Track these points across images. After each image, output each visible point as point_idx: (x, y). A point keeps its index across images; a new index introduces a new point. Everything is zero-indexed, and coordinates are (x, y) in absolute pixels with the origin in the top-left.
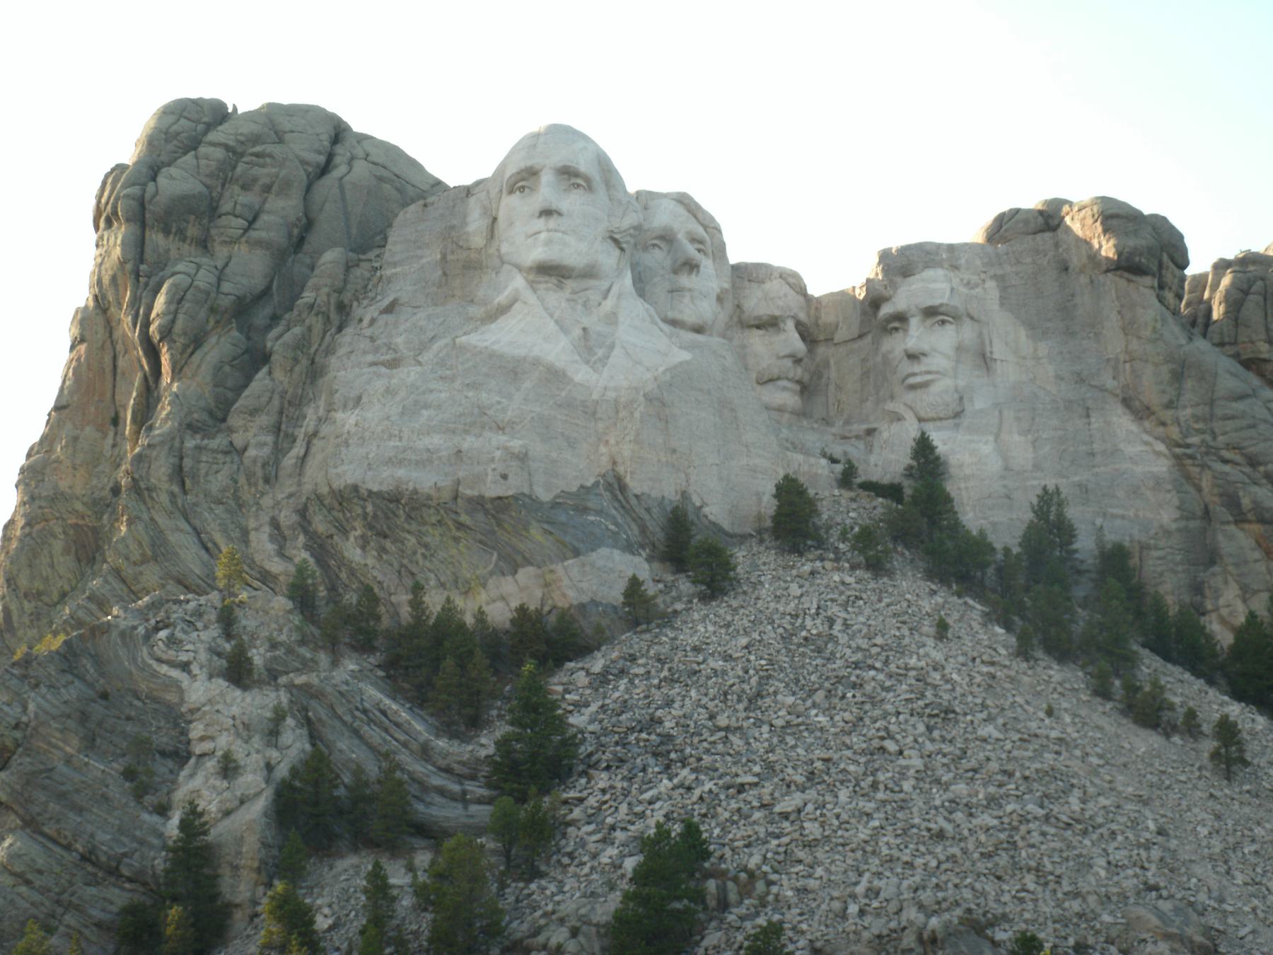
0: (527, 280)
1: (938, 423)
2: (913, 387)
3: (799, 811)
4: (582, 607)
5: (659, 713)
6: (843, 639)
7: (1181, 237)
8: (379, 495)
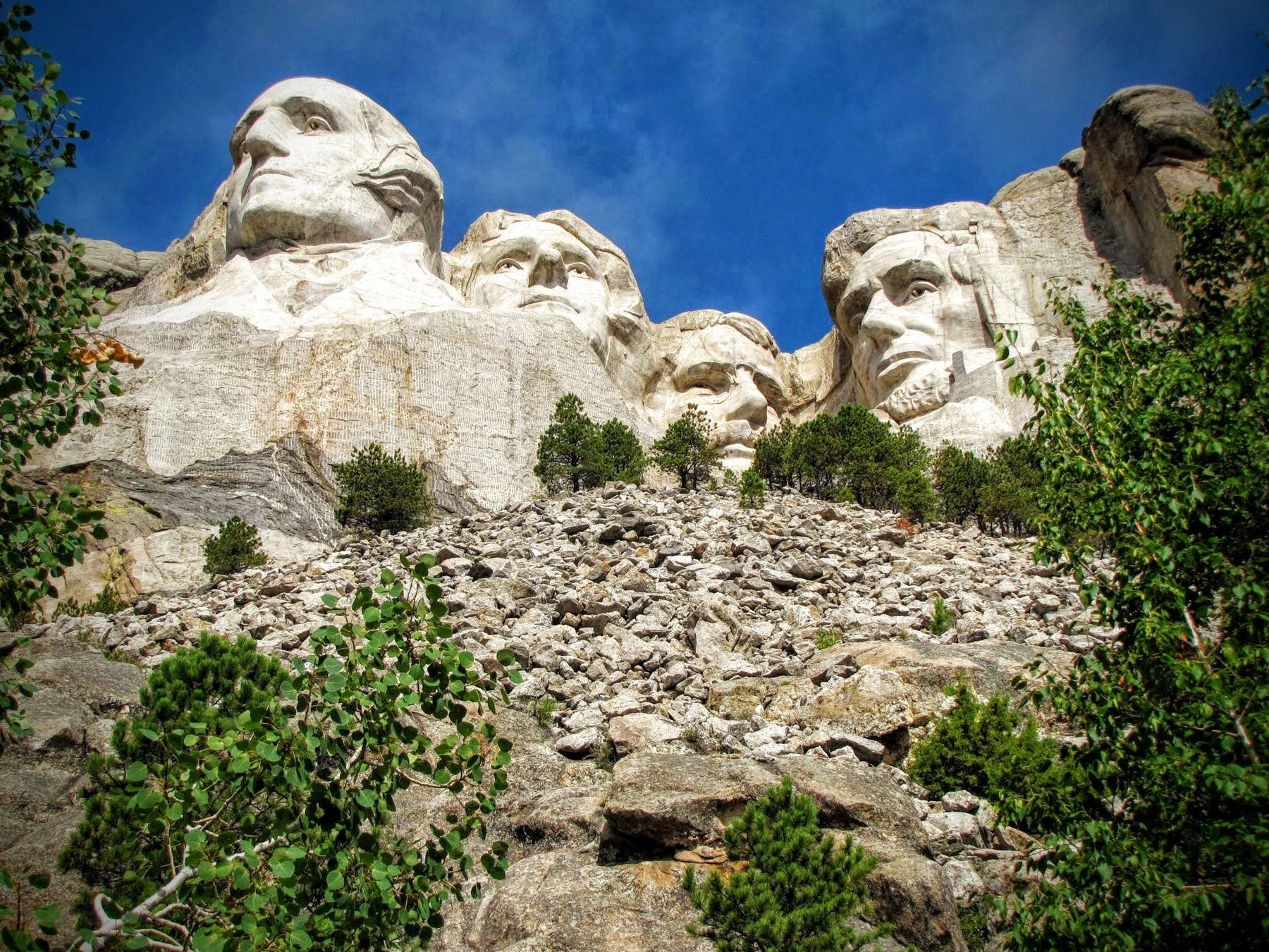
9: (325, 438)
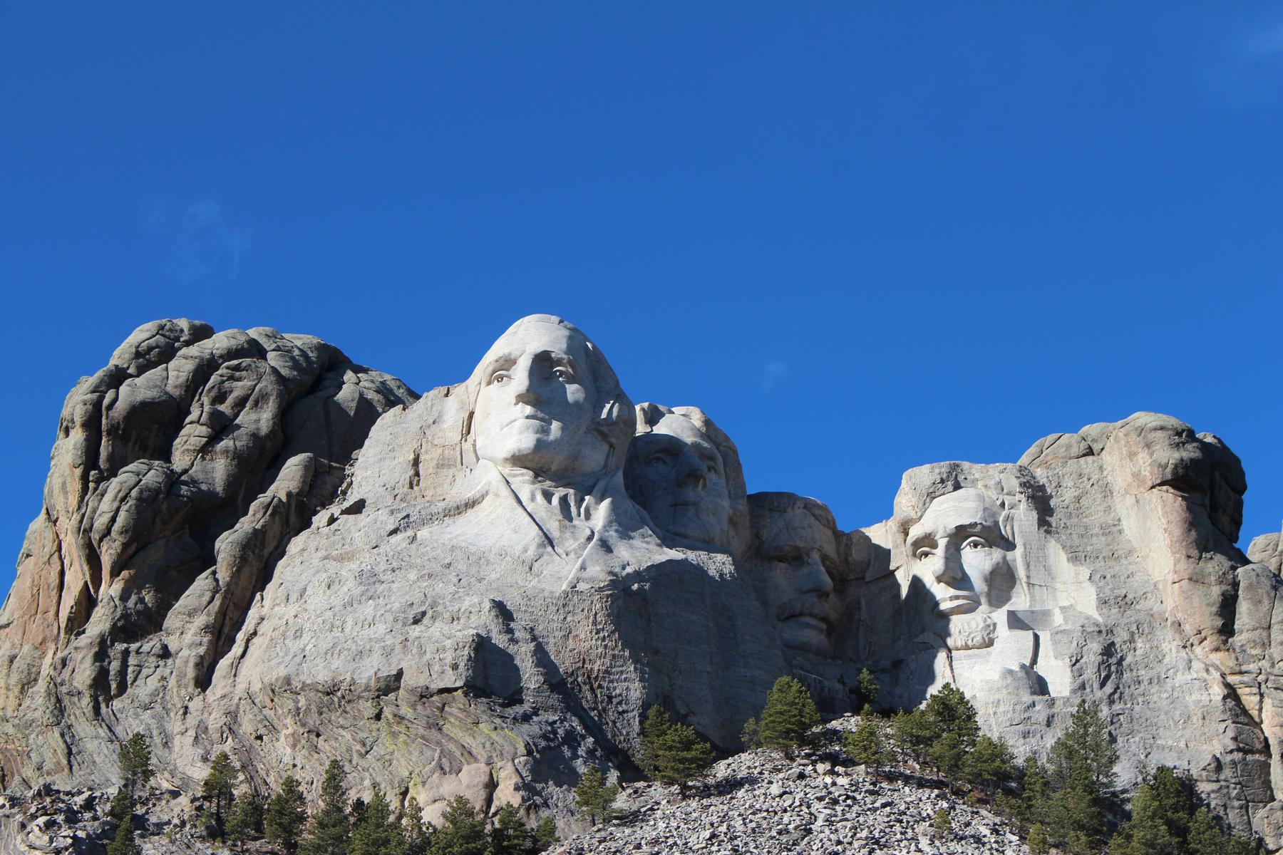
7: (1238, 461)
8: (312, 687)
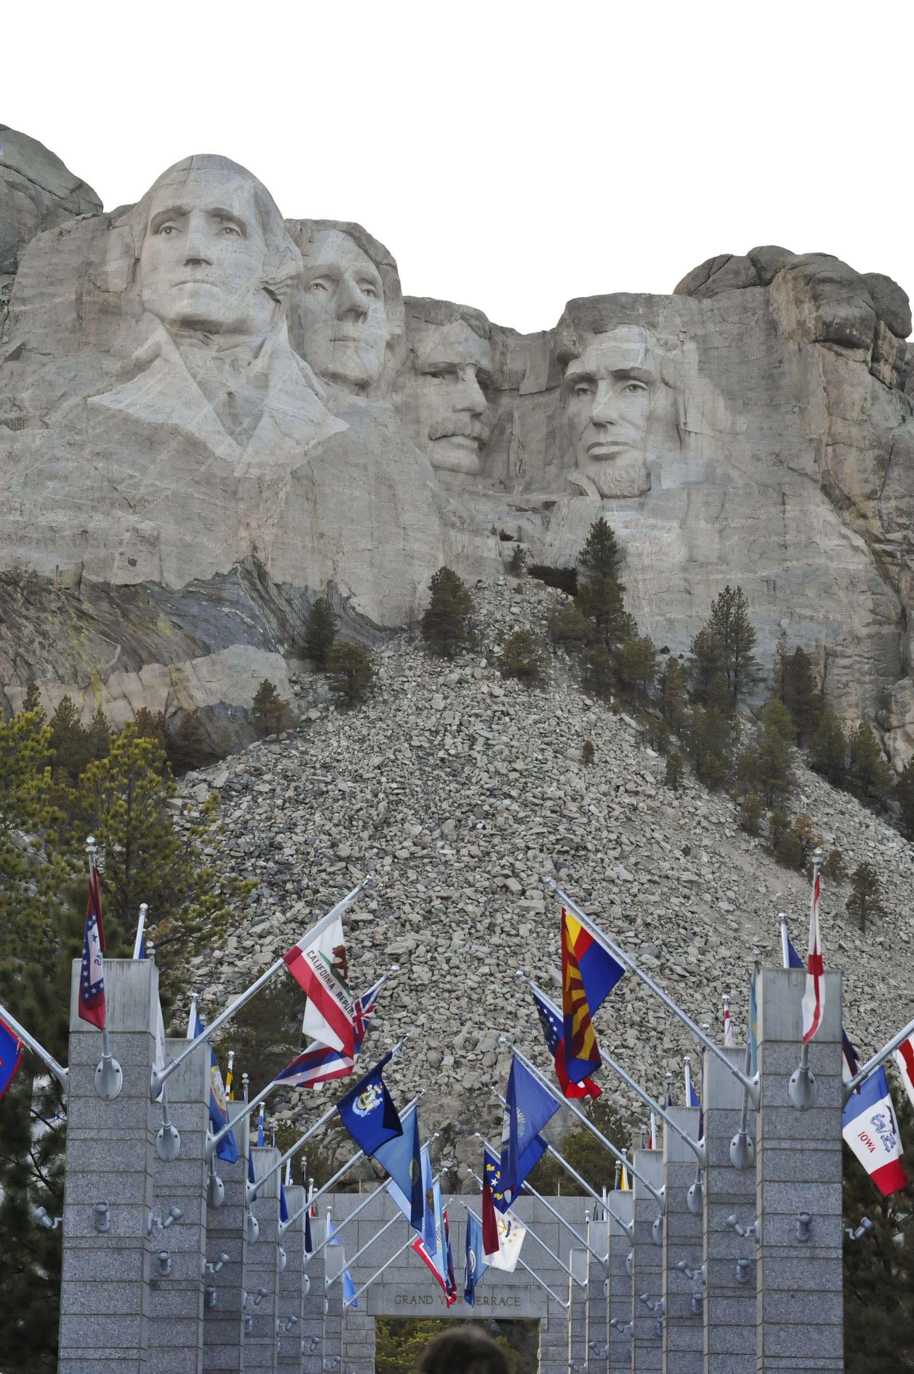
0: (170, 333)
1: (622, 502)
2: (598, 458)
3: (411, 953)
4: (210, 709)
5: (279, 838)
6: (482, 761)
9: (269, 563)
